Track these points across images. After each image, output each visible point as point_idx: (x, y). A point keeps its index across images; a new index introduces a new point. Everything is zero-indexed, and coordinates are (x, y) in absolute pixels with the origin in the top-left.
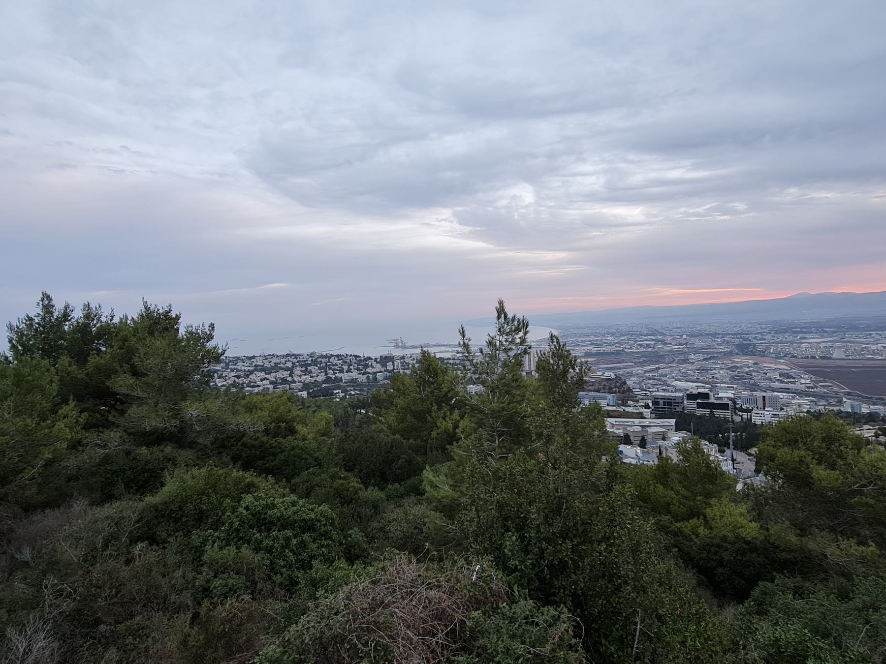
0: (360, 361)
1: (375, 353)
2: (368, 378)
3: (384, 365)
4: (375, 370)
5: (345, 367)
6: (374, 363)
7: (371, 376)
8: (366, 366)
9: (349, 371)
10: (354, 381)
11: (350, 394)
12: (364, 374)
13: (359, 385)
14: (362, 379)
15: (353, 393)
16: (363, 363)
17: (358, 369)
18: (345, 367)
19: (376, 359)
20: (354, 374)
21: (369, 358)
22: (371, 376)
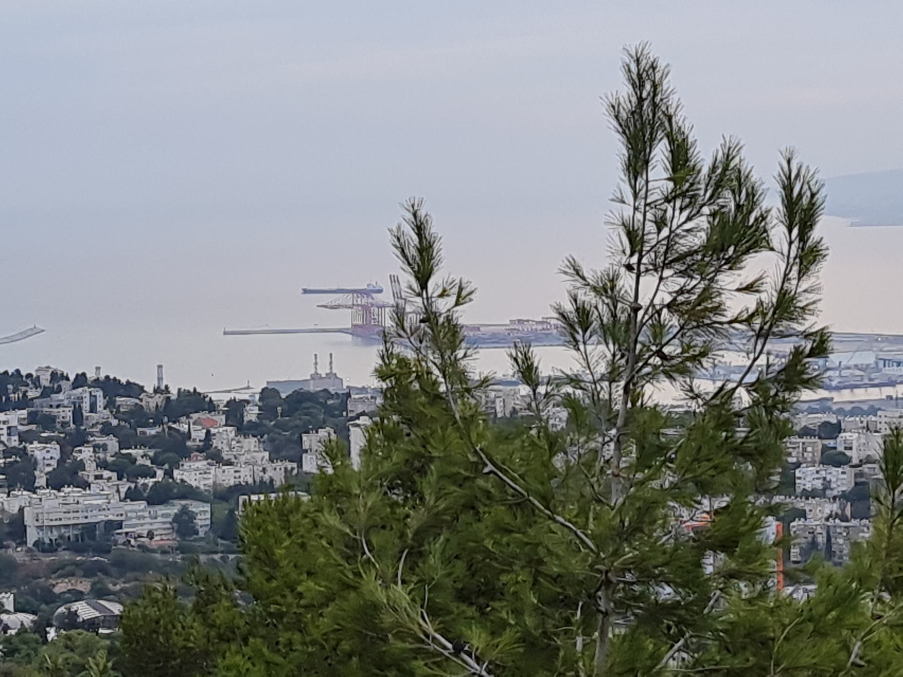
0: (139, 416)
1: (234, 374)
2: (183, 524)
3: (286, 448)
4: (227, 477)
5: (46, 455)
6: (224, 436)
7: (202, 513)
8: (176, 450)
9: (67, 476)
10: (92, 538)
11: (71, 621)
12: (158, 497)
13: (123, 566)
14: (149, 523)
15: (84, 611)
16: (151, 427)
17: (124, 468)
18: (46, 455)
19: (234, 410)
20: (100, 500)
21: (195, 402)
22: (202, 513)
